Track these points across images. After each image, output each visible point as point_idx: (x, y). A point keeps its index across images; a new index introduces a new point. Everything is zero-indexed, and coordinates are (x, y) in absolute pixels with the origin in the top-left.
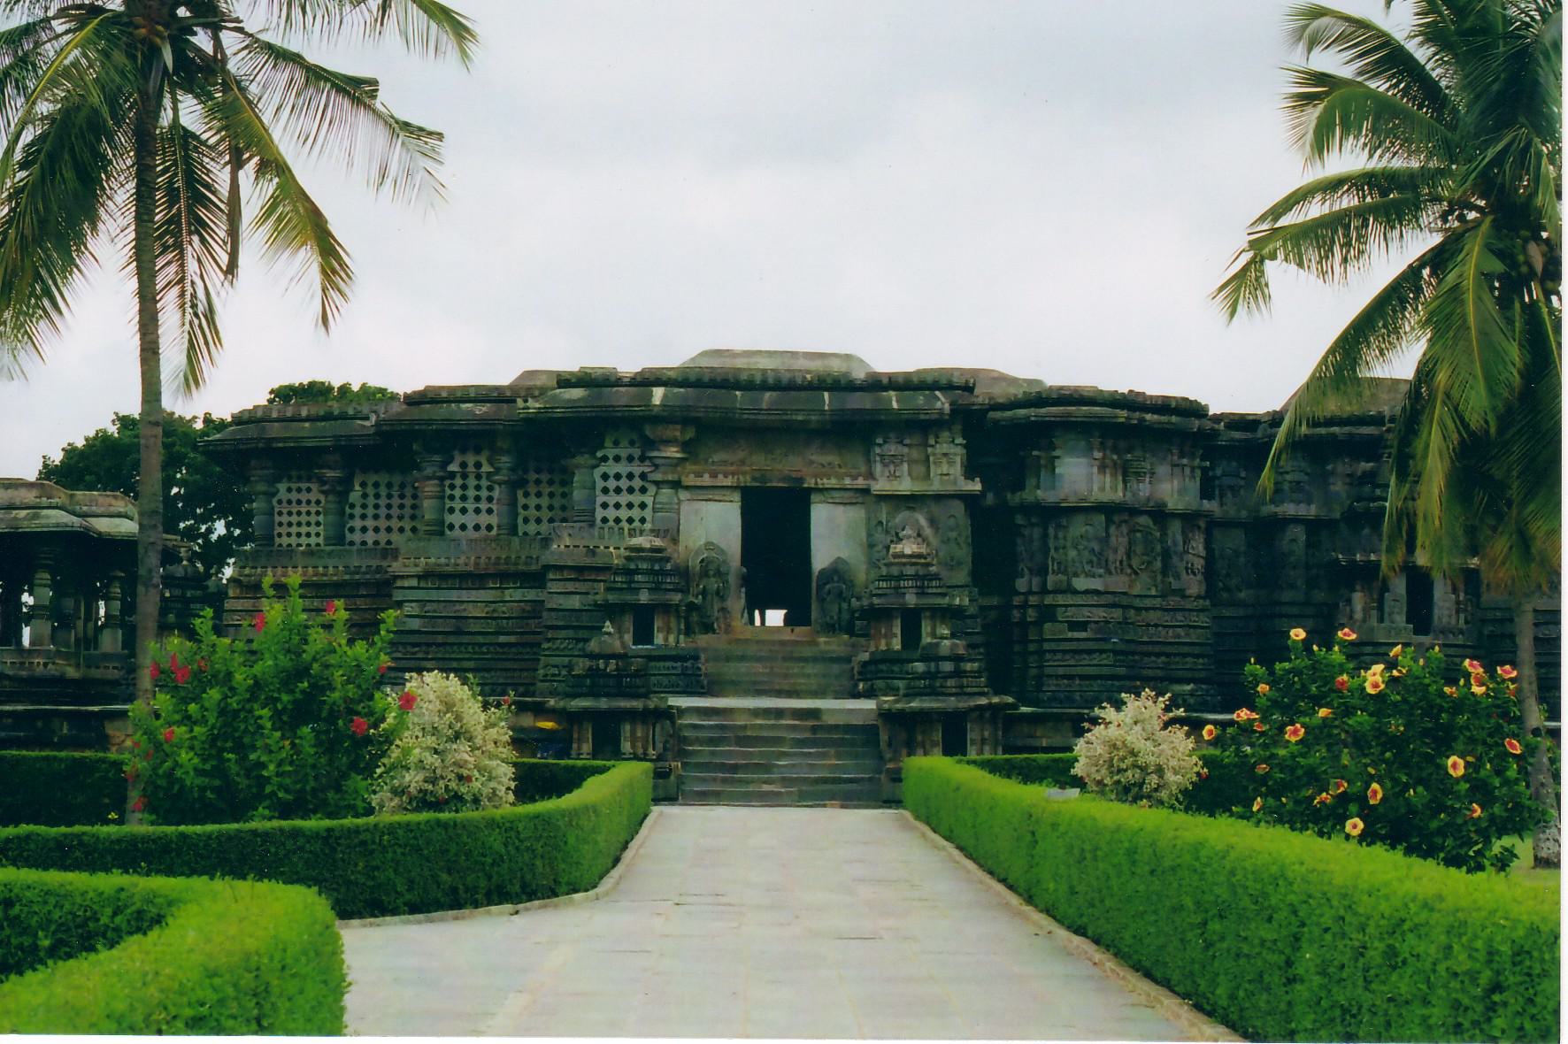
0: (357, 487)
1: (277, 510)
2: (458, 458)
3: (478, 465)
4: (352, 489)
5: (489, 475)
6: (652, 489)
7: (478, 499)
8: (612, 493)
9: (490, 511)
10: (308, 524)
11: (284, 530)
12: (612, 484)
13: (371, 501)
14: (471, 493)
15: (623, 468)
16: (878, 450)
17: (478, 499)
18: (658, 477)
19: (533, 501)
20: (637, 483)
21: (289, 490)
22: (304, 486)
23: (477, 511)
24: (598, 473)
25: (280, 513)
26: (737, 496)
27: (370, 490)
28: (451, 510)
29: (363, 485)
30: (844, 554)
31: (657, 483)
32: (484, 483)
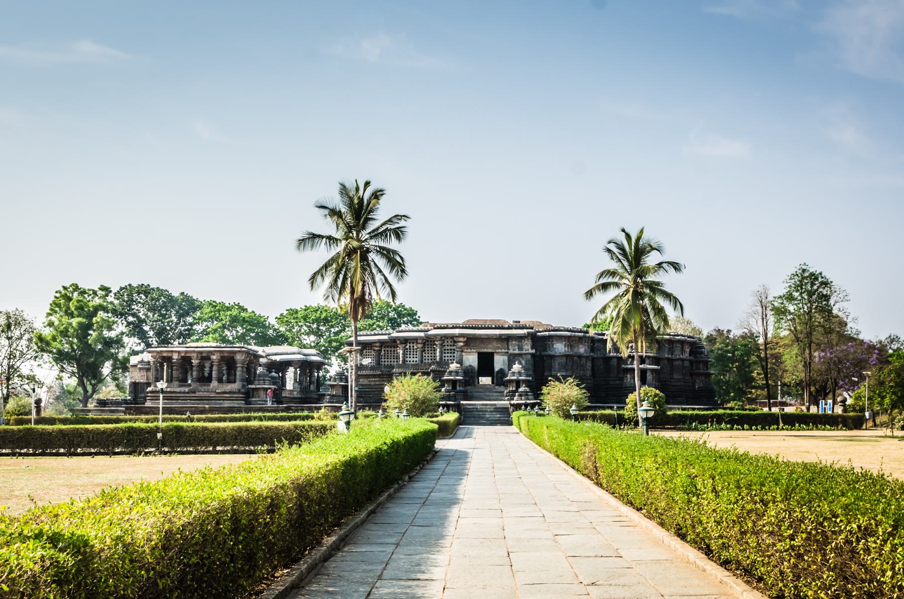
2: (408, 345)
3: (413, 347)
5: (416, 349)
7: (413, 354)
12: (446, 351)
13: (386, 355)
14: (412, 353)
15: (448, 348)
17: (413, 354)
18: (458, 350)
19: (427, 355)
20: (452, 351)
22: (370, 351)
24: (443, 349)
26: (477, 354)
27: (386, 352)
29: (384, 351)
30: (502, 367)
32: (415, 351)
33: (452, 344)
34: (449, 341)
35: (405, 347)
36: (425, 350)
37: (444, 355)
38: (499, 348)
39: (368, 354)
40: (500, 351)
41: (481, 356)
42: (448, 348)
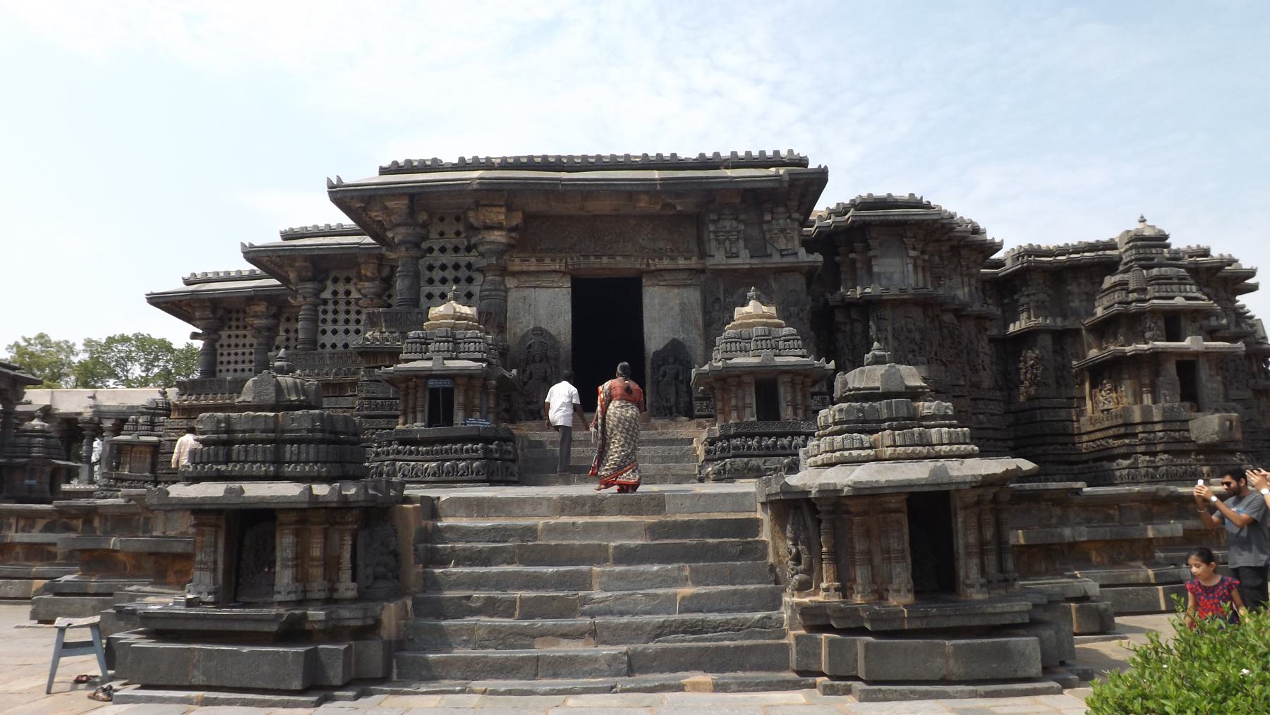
0: (282, 333)
1: (219, 352)
2: (330, 287)
3: (348, 293)
4: (277, 335)
6: (479, 278)
7: (347, 321)
8: (437, 283)
10: (243, 362)
11: (224, 368)
12: (437, 275)
14: (342, 317)
15: (448, 259)
16: (712, 228)
17: (347, 321)
18: (483, 263)
20: (463, 273)
21: (230, 336)
22: (241, 332)
23: (347, 332)
24: (423, 263)
25: (222, 354)
28: (324, 332)
29: (287, 331)
31: (481, 270)
32: (353, 308)
34: (450, 232)
35: (317, 294)
37: (426, 289)
38: (660, 255)
42: (448, 259)
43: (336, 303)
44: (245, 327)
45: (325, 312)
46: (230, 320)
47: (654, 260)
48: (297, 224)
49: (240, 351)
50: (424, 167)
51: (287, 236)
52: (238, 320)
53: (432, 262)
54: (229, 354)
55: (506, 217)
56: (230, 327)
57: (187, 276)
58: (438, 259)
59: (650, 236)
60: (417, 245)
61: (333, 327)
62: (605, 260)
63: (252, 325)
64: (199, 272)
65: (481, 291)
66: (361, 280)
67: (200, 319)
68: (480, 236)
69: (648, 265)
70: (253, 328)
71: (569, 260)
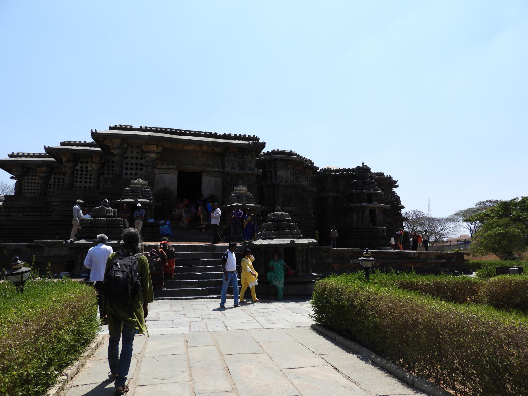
1: (24, 185)
3: (87, 167)
4: (50, 179)
5: (91, 171)
6: (145, 168)
7: (86, 178)
9: (90, 182)
10: (34, 190)
11: (25, 191)
12: (129, 166)
14: (84, 176)
17: (86, 178)
20: (139, 167)
22: (34, 178)
23: (86, 182)
25: (25, 186)
27: (57, 180)
28: (76, 182)
29: (55, 178)
32: (89, 173)
33: (139, 156)
36: (104, 174)
37: (125, 171)
39: (30, 181)
40: (211, 169)
41: (183, 176)
42: (134, 161)
43: (82, 171)
44: (36, 176)
45: (77, 174)
46: (29, 172)
47: (207, 168)
48: (67, 140)
49: (33, 185)
50: (126, 128)
51: (62, 144)
52: (33, 172)
53: (128, 162)
54: (28, 186)
55: (156, 149)
56: (29, 175)
57: (10, 153)
58: (130, 161)
59: (206, 159)
60: (122, 156)
61: (80, 180)
62: (190, 166)
63: (39, 175)
64: (16, 152)
65: (145, 174)
66: (93, 163)
67: (15, 171)
68: (147, 155)
69: (205, 169)
70: (40, 177)
71: (178, 166)
